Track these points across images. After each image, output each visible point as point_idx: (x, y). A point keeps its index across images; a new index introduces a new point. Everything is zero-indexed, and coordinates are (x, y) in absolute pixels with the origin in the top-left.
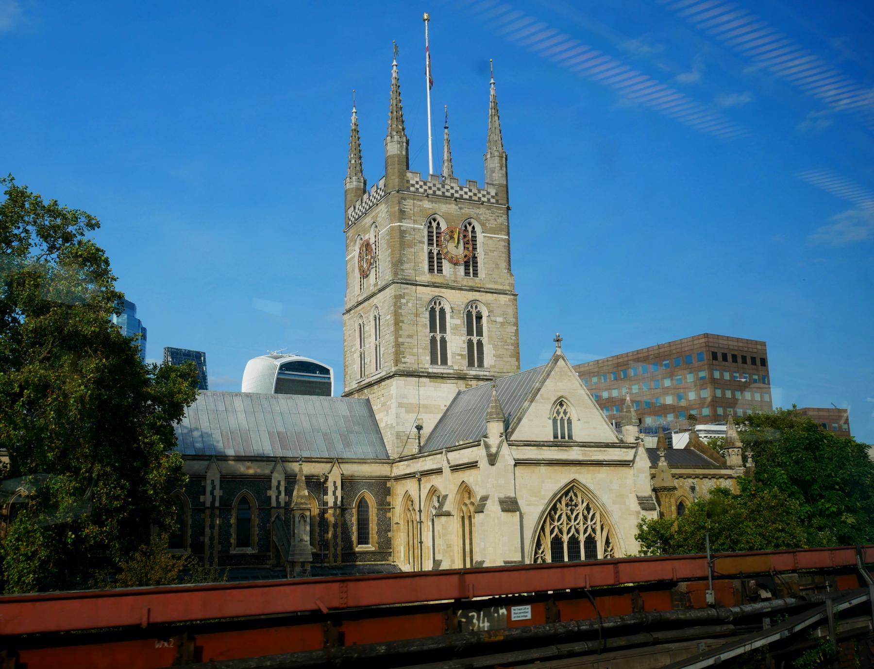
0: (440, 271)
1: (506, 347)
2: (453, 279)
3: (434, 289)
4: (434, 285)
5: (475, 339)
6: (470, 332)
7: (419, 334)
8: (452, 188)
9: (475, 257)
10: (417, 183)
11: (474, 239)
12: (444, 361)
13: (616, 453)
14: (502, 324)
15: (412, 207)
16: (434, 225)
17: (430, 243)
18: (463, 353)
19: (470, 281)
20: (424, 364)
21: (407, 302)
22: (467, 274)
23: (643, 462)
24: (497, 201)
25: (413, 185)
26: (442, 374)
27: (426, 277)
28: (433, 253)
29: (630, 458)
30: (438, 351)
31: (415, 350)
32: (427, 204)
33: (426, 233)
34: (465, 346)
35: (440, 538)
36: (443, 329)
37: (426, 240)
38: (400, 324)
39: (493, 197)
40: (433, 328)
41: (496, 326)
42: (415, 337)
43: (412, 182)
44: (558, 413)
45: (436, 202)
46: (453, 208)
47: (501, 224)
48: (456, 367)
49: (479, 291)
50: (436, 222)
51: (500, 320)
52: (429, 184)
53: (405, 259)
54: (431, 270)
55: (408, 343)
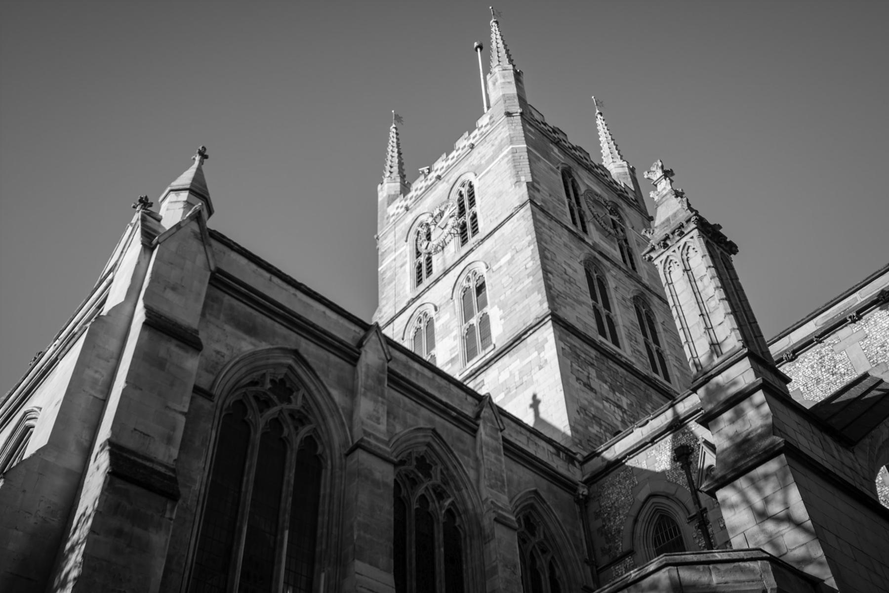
1: (518, 290)
5: (474, 321)
18: (453, 356)
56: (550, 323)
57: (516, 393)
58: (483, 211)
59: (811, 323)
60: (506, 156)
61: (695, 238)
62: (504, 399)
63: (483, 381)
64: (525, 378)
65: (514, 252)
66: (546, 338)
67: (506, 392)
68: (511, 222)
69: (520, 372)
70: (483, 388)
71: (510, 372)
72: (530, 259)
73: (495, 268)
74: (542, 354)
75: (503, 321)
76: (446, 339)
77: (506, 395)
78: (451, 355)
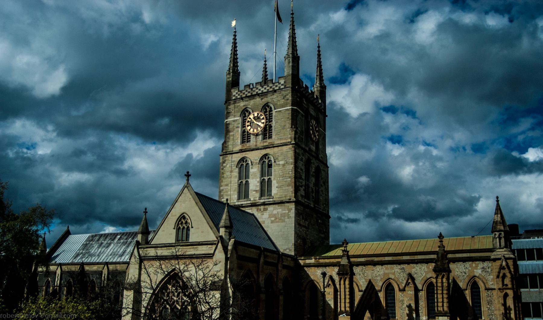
1: (285, 180)
3: (242, 153)
4: (241, 151)
5: (266, 178)
7: (232, 182)
8: (257, 89)
9: (271, 127)
11: (271, 115)
12: (247, 196)
13: (204, 249)
14: (284, 165)
15: (233, 109)
17: (243, 126)
18: (257, 189)
20: (234, 200)
21: (227, 165)
22: (264, 138)
23: (220, 255)
26: (242, 204)
27: (238, 147)
29: (212, 252)
31: (229, 193)
32: (242, 104)
34: (259, 184)
36: (247, 176)
37: (240, 125)
38: (222, 179)
39: (282, 85)
41: (280, 168)
42: (230, 185)
44: (182, 223)
46: (258, 100)
49: (269, 148)
51: (282, 163)
52: (243, 92)
54: (243, 142)
55: (226, 189)
56: (294, 203)
57: (278, 221)
58: (276, 130)
59: (364, 258)
60: (287, 110)
61: (349, 277)
62: (274, 220)
63: (267, 208)
64: (282, 218)
65: (285, 162)
66: (292, 208)
67: (275, 218)
68: (287, 147)
69: (281, 215)
70: (267, 211)
71: (278, 212)
72: (291, 170)
73: (277, 163)
74: (289, 213)
75: (277, 189)
76: (254, 180)
77: (275, 219)
78: (256, 188)
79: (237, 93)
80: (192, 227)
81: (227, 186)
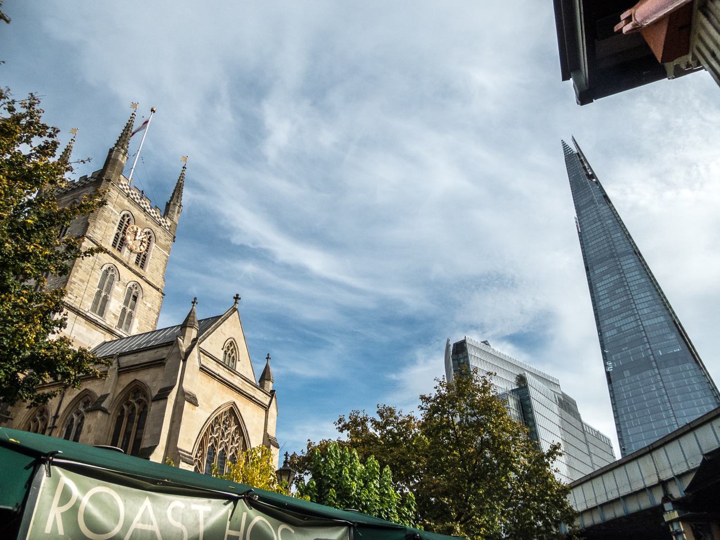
0: (119, 250)
2: (127, 260)
6: (126, 303)
7: (90, 283)
10: (125, 185)
13: (261, 396)
15: (116, 197)
16: (127, 219)
18: (117, 314)
19: (137, 269)
20: (85, 307)
24: (170, 230)
25: (122, 185)
28: (118, 236)
30: (101, 304)
32: (126, 202)
33: (119, 219)
35: (89, 432)
37: (118, 223)
40: (101, 286)
42: (86, 284)
43: (122, 182)
45: (132, 205)
47: (168, 246)
48: (108, 322)
50: (128, 218)
51: (149, 305)
53: (99, 227)
79: (125, 185)
80: (239, 361)
81: (81, 281)
